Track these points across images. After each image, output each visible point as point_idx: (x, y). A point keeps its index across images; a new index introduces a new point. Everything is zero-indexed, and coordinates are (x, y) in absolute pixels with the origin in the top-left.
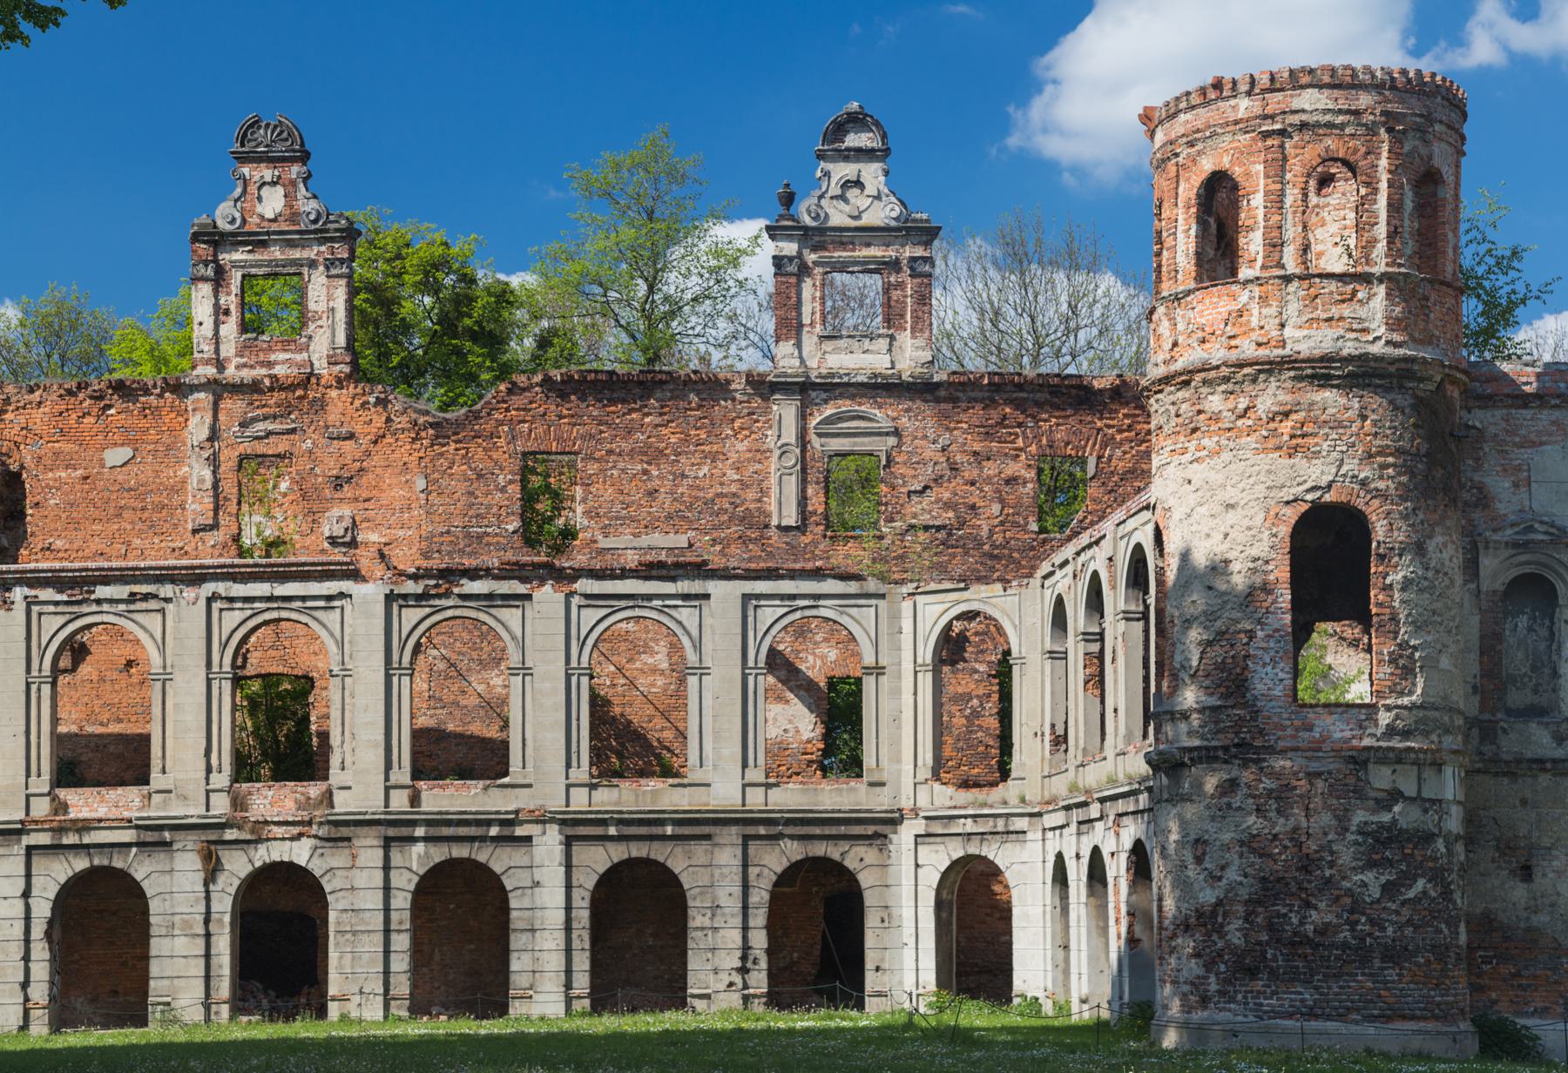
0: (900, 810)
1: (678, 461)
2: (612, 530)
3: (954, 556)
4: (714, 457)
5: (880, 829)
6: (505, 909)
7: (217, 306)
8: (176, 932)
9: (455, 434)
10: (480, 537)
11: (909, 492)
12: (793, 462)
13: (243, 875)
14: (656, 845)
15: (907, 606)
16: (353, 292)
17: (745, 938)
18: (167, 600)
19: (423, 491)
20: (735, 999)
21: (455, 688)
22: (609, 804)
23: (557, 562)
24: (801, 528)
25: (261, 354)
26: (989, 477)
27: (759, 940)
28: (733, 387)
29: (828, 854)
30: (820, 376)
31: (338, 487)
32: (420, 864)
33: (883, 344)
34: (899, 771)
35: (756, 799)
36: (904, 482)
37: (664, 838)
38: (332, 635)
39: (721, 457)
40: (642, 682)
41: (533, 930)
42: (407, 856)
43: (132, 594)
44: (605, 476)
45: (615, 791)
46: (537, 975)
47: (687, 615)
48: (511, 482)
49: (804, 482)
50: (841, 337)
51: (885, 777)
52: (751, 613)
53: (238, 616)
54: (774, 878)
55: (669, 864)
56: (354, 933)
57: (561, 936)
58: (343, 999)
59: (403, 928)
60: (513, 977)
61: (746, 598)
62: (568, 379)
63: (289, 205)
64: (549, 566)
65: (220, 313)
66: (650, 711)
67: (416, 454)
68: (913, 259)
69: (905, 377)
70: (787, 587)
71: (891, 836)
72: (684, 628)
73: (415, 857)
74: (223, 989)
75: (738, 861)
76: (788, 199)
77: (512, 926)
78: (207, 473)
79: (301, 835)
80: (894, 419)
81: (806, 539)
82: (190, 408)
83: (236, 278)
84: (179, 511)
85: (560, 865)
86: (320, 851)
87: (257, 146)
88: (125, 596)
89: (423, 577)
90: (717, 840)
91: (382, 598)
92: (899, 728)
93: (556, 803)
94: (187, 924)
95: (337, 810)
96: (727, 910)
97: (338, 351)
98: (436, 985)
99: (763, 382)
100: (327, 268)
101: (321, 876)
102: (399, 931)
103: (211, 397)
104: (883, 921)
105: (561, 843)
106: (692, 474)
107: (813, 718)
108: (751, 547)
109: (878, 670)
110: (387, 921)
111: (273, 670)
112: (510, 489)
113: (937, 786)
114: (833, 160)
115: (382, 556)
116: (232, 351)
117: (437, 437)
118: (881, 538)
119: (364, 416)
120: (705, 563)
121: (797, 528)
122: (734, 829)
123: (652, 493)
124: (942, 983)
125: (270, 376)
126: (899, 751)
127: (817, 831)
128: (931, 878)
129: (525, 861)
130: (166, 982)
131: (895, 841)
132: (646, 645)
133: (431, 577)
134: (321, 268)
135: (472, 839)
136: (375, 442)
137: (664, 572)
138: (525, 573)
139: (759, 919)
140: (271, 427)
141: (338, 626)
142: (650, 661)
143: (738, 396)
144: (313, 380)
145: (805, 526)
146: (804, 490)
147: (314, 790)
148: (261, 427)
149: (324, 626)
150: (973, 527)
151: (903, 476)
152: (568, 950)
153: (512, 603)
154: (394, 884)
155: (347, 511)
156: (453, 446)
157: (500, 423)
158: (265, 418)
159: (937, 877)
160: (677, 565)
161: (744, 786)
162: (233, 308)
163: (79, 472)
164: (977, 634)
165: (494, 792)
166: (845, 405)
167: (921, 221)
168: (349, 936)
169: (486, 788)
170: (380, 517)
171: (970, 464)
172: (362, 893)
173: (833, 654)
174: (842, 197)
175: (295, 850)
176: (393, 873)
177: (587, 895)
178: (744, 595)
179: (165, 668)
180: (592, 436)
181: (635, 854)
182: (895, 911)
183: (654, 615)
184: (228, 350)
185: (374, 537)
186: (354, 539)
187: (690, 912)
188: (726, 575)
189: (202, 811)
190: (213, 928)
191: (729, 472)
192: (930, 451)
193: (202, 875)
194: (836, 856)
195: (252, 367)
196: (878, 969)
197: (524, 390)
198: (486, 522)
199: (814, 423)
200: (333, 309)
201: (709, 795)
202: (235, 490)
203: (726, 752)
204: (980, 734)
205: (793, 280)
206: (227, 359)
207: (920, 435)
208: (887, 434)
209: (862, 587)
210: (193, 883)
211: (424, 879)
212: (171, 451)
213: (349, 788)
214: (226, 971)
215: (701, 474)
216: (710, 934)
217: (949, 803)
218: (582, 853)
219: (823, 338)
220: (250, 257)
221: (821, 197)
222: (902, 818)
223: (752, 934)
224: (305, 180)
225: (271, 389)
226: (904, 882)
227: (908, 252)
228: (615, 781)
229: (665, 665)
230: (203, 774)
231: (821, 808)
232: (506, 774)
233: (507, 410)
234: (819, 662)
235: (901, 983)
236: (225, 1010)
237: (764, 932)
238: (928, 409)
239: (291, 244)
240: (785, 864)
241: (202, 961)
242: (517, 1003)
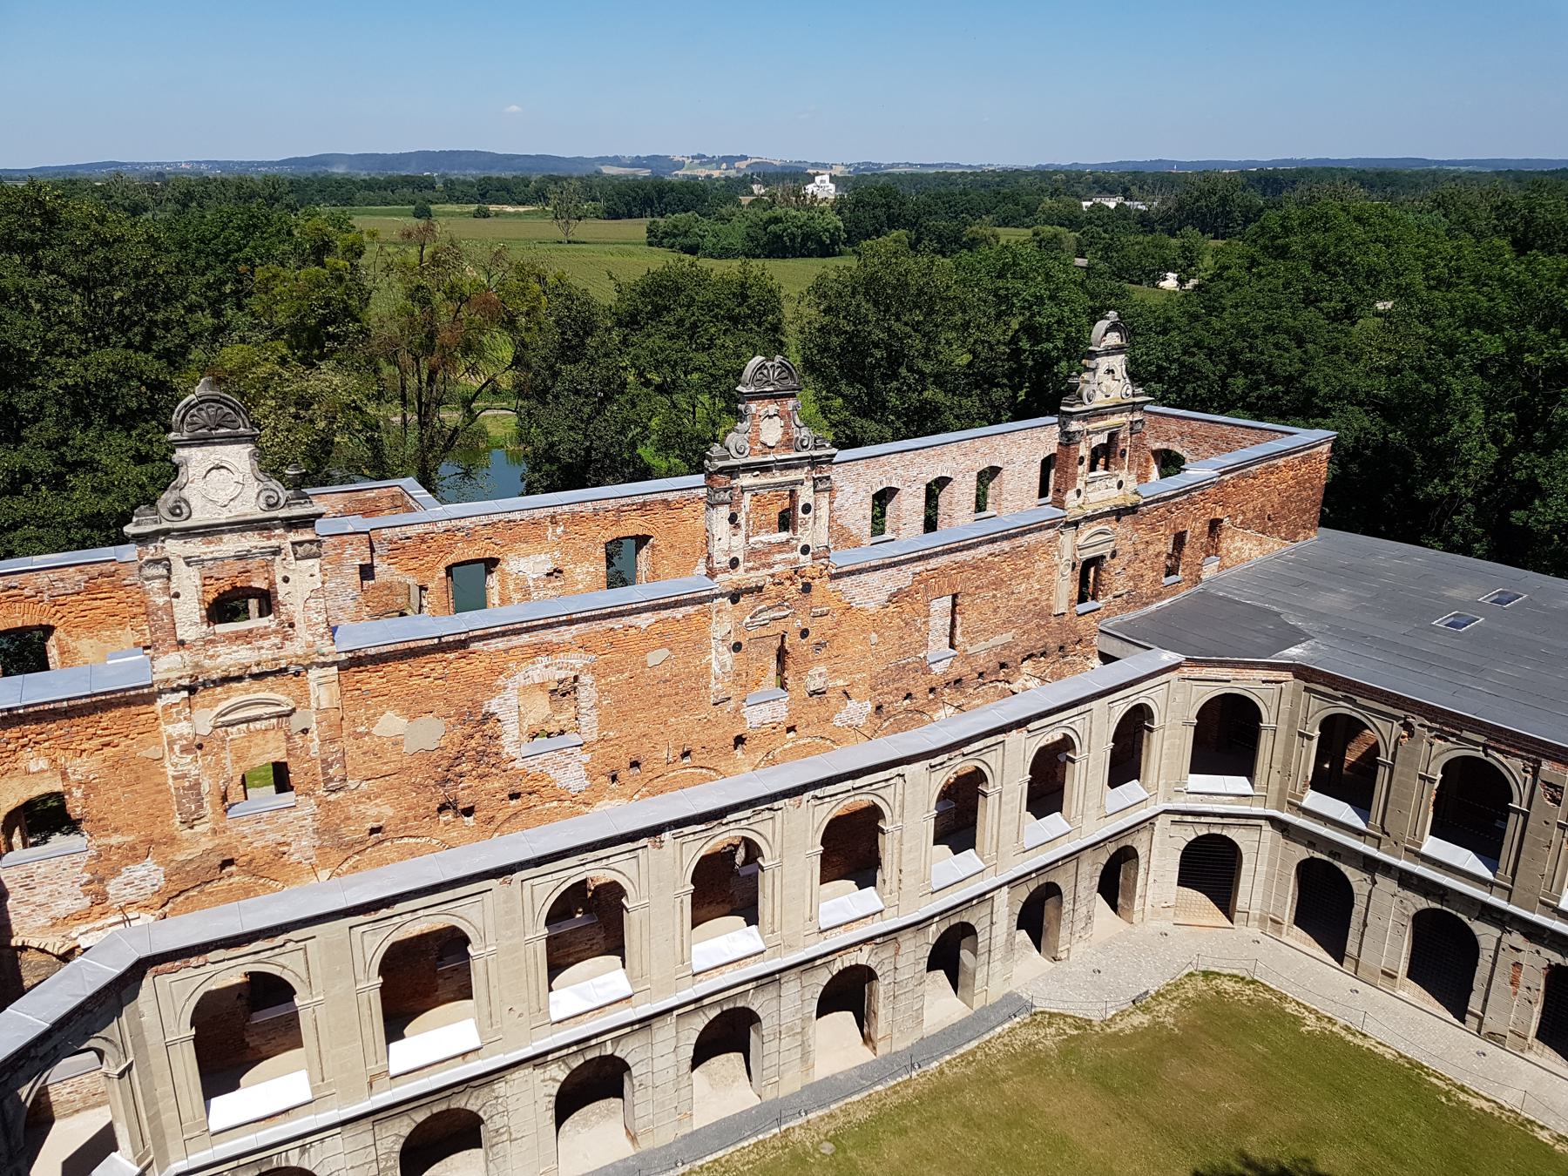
4: (1027, 577)
25: (763, 557)
73: (931, 933)
106: (1017, 591)
123: (995, 611)
148: (766, 615)
155: (823, 669)
163: (627, 674)
185: (840, 682)
195: (758, 569)
211: (934, 946)
212: (700, 645)
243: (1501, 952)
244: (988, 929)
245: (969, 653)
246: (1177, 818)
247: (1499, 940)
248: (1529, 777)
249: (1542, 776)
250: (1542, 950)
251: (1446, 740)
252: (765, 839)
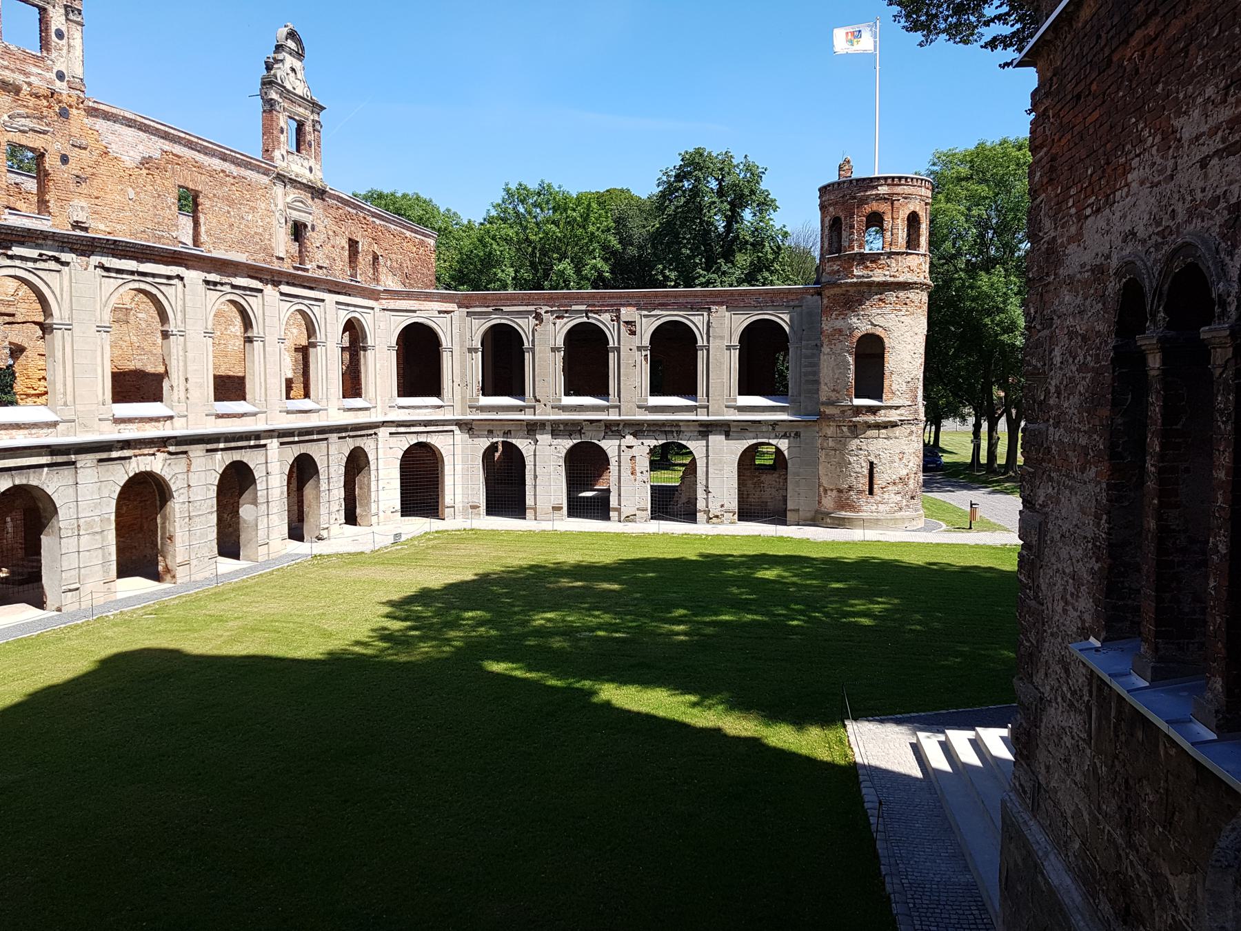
4: (253, 209)
18: (67, 264)
32: (220, 467)
43: (41, 255)
73: (217, 461)
86: (169, 462)
88: (36, 256)
101: (170, 480)
141: (174, 298)
243: (622, 453)
244: (265, 478)
246: (393, 430)
247: (620, 446)
248: (615, 323)
249: (623, 318)
250: (644, 441)
251: (562, 317)
252: (53, 292)
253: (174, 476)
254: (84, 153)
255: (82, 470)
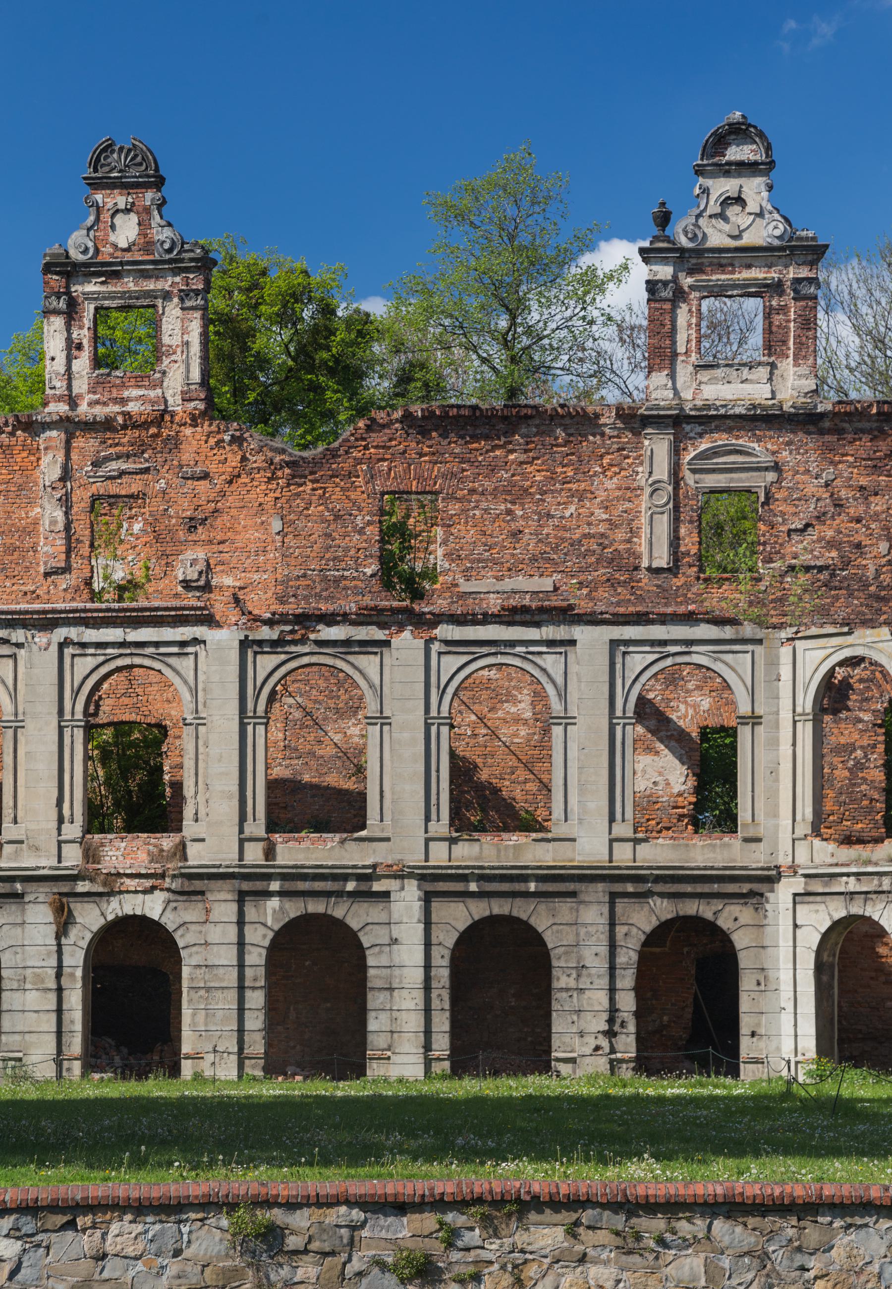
0: (777, 867)
1: (544, 501)
2: (474, 573)
3: (837, 598)
5: (756, 887)
6: (362, 967)
7: (69, 340)
8: (28, 986)
9: (312, 473)
10: (337, 581)
11: (790, 531)
12: (665, 500)
13: (95, 928)
14: (518, 901)
15: (785, 652)
16: (207, 322)
17: (612, 1000)
18: (19, 645)
19: (278, 533)
20: (601, 1064)
21: (311, 737)
22: (470, 859)
23: (416, 607)
24: (673, 570)
25: (114, 390)
26: (877, 514)
27: (627, 1002)
28: (603, 421)
29: (701, 913)
30: (695, 408)
31: (192, 529)
32: (275, 919)
33: (763, 372)
34: (777, 827)
35: (623, 854)
36: (784, 520)
37: (527, 895)
38: (186, 682)
39: (589, 495)
40: (505, 732)
41: (391, 989)
42: (262, 911)
44: (467, 517)
45: (476, 847)
46: (395, 1035)
47: (552, 662)
48: (369, 523)
49: (676, 521)
50: (718, 366)
51: (761, 832)
52: (619, 659)
53: (90, 662)
54: (643, 938)
55: (533, 921)
56: (208, 989)
57: (419, 995)
58: (196, 1057)
59: (258, 984)
60: (370, 1038)
61: (614, 644)
62: (429, 415)
63: (142, 234)
64: (408, 611)
65: (72, 347)
66: (513, 762)
67: (272, 495)
68: (797, 281)
69: (786, 407)
70: (658, 632)
71: (768, 894)
72: (549, 676)
73: (269, 912)
74: (75, 1045)
75: (604, 920)
76: (664, 219)
77: (369, 985)
78: (59, 515)
79: (153, 889)
80: (774, 453)
81: (678, 582)
82: (42, 447)
83: (89, 310)
84: (31, 553)
85: (419, 921)
86: (173, 905)
87: (110, 171)
89: (278, 623)
90: (583, 897)
91: (236, 644)
92: (777, 780)
93: (415, 858)
94: (39, 979)
95: (190, 863)
96: (593, 971)
97: (193, 387)
98: (292, 1044)
99: (635, 416)
100: (182, 300)
102: (254, 988)
103: (63, 436)
104: (759, 984)
105: (420, 899)
106: (558, 514)
107: (684, 770)
108: (619, 590)
109: (754, 720)
110: (241, 977)
111: (126, 717)
112: (368, 530)
113: (817, 842)
114: (713, 175)
115: (237, 600)
116: (85, 387)
117: (294, 477)
118: (759, 580)
119: (220, 455)
120: (571, 607)
121: (669, 570)
122: (600, 886)
123: (516, 534)
124: (821, 1050)
125: (124, 414)
126: (777, 805)
127: (689, 888)
128: (810, 939)
129: (383, 918)
130: (17, 1037)
131: (771, 900)
132: (509, 694)
133: (286, 623)
134: (176, 300)
135: (328, 894)
136: (230, 482)
137: (528, 617)
138: (383, 619)
139: (627, 980)
140: (124, 467)
141: (192, 673)
142: (513, 710)
143: (607, 431)
144: (167, 418)
145: (677, 567)
146: (676, 530)
147: (167, 842)
148: (114, 465)
149: (178, 673)
150: (858, 567)
151: (783, 514)
152: (427, 1010)
153: (370, 649)
154: (248, 939)
155: (200, 554)
156: (310, 486)
157: (359, 461)
158: (118, 457)
159: (816, 939)
160: (542, 610)
161: (611, 841)
162: (85, 342)
164: (861, 681)
165: (351, 846)
166: (722, 439)
167: (807, 239)
168: (202, 992)
169: (343, 842)
170: (234, 560)
171: (855, 499)
172: (215, 948)
173: (706, 703)
174: (722, 216)
175: (148, 904)
176: (247, 929)
177: (447, 953)
178: (611, 641)
179: (16, 715)
180: (453, 475)
181: (496, 911)
182: (771, 974)
183: (517, 662)
184: (80, 386)
185: (228, 581)
186: (208, 582)
187: (554, 972)
188: (592, 619)
189: (54, 863)
190: (64, 982)
191: (597, 511)
192: (812, 487)
193: (54, 928)
194: (708, 915)
195: (105, 404)
196: (753, 1034)
197: (384, 426)
198: (343, 565)
199: (688, 458)
200: (187, 343)
201: (574, 850)
202: (87, 532)
203: (591, 805)
204: (864, 787)
205: (667, 306)
206: (80, 396)
207: (802, 469)
208: (767, 469)
209: (737, 632)
210: (45, 936)
211: (278, 934)
213: (203, 840)
214: (78, 1027)
215: (567, 514)
216: (575, 995)
217: (830, 860)
218: (443, 911)
219: (698, 367)
220: (103, 288)
221: (698, 216)
222: (779, 877)
223: (619, 996)
224: (160, 207)
225: (124, 427)
226: (781, 943)
227: (792, 273)
228: (476, 835)
229: (528, 714)
230: (55, 825)
231: (693, 865)
232: (363, 827)
233: (366, 448)
234: (691, 712)
235: (778, 1049)
236: (77, 1066)
237: (632, 994)
238: (811, 442)
239: (145, 275)
240: (655, 922)
241: (54, 1016)
242: (374, 1064)
245: (462, 589)
253: (181, 926)
254: (203, 485)
255: (31, 905)
